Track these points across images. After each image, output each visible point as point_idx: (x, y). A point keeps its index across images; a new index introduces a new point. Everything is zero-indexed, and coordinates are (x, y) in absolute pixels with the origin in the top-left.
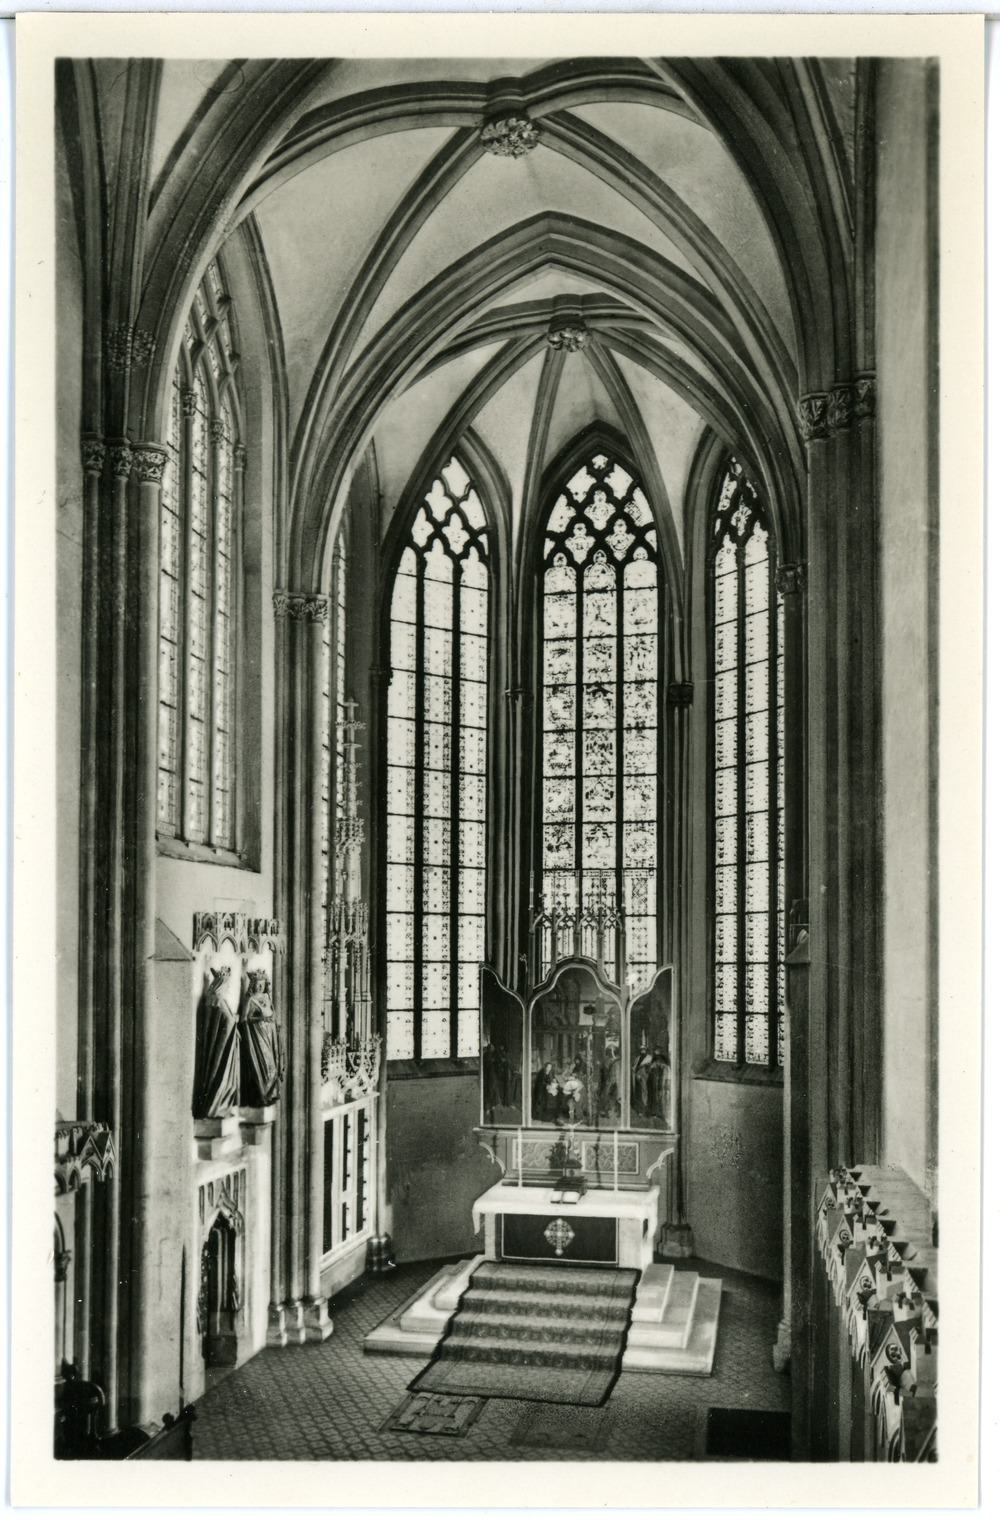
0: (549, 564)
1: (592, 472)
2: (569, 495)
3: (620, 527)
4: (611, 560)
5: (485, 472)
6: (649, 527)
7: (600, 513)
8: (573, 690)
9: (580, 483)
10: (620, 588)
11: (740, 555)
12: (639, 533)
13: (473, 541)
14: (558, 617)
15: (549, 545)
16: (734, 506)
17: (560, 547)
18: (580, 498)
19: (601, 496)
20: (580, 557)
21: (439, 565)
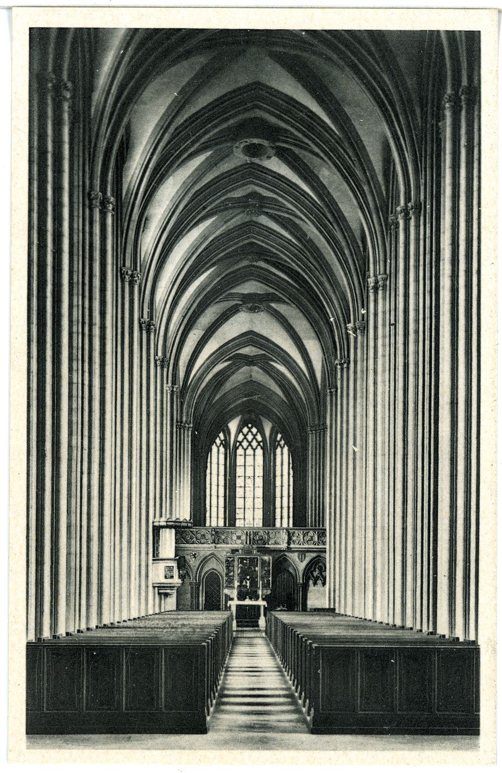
0: (238, 448)
1: (248, 427)
2: (242, 432)
3: (254, 441)
4: (252, 448)
6: (261, 442)
7: (250, 437)
8: (243, 478)
9: (245, 430)
10: (254, 455)
12: (259, 443)
13: (221, 443)
14: (240, 461)
15: (238, 444)
16: (281, 440)
17: (240, 444)
18: (245, 433)
19: (250, 434)
20: (245, 447)
21: (214, 448)
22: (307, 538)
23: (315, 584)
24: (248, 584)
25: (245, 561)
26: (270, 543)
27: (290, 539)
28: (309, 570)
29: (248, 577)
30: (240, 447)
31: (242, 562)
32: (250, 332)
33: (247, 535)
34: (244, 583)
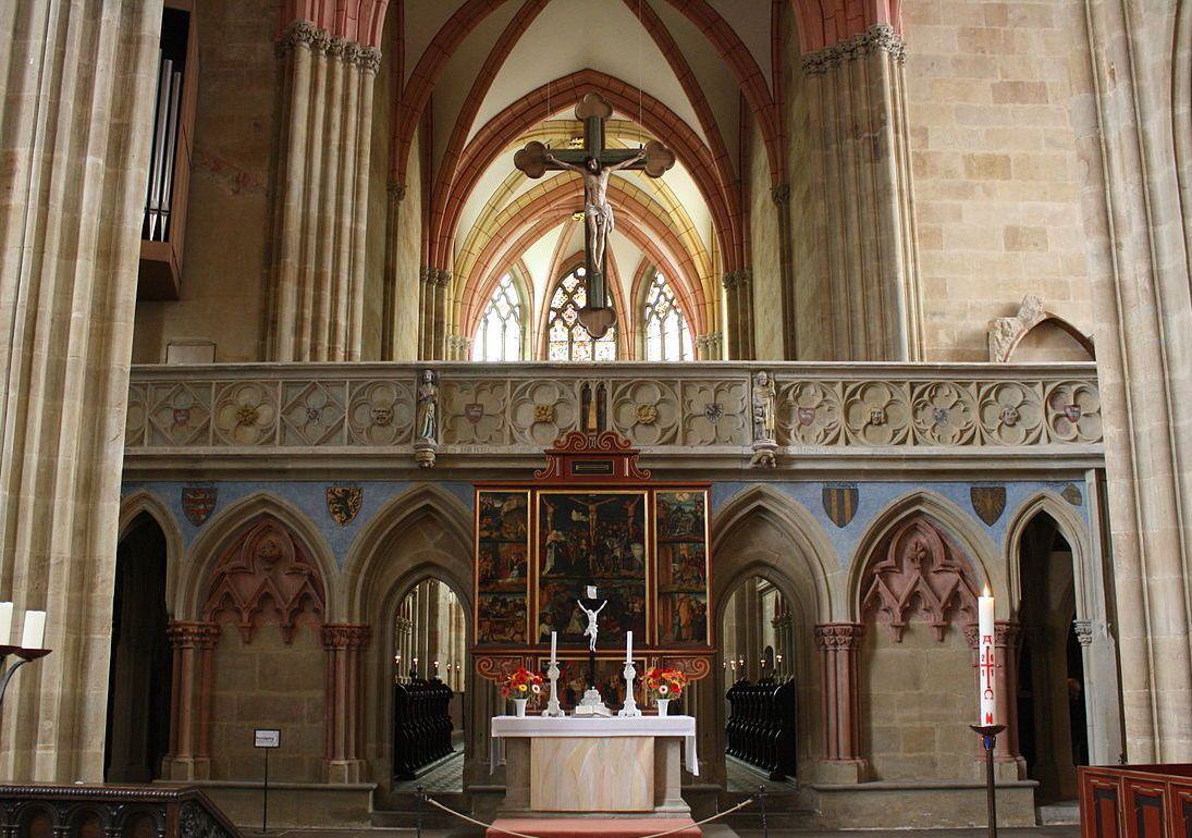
0: (553, 325)
2: (564, 288)
5: (519, 274)
9: (570, 282)
11: (661, 327)
18: (570, 290)
21: (494, 322)
22: (866, 410)
23: (903, 630)
24: (593, 630)
25: (575, 516)
26: (694, 436)
27: (784, 412)
28: (871, 564)
29: (592, 592)
30: (559, 324)
31: (561, 521)
32: (587, 73)
33: (585, 401)
34: (575, 626)
